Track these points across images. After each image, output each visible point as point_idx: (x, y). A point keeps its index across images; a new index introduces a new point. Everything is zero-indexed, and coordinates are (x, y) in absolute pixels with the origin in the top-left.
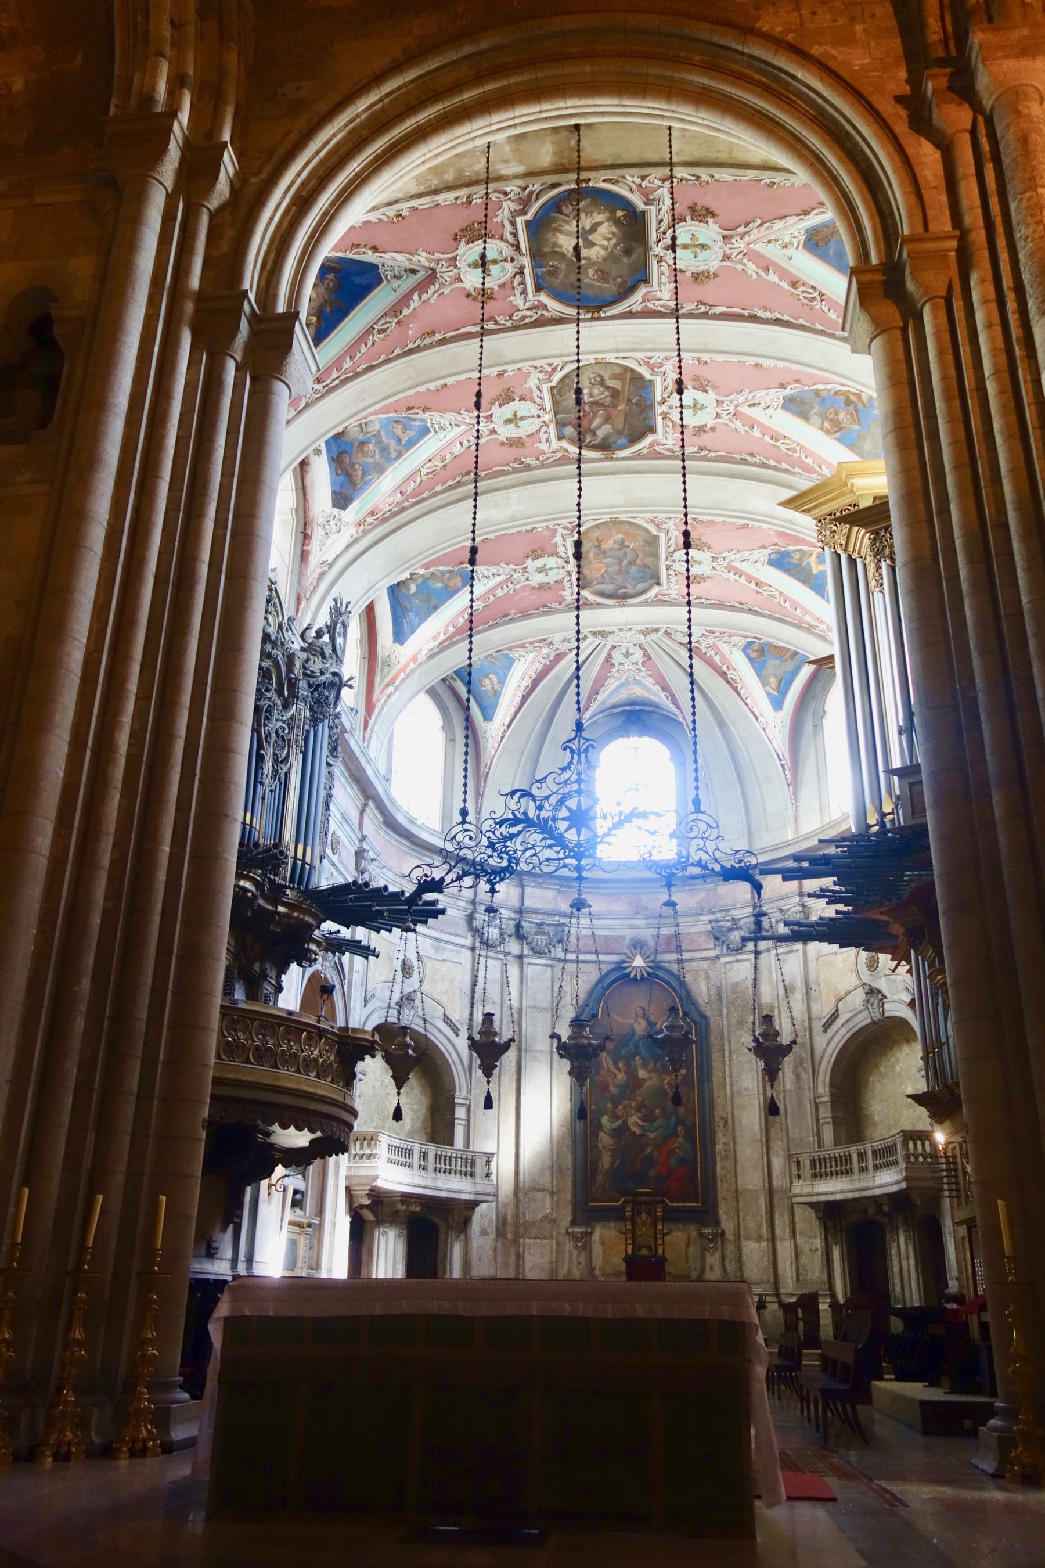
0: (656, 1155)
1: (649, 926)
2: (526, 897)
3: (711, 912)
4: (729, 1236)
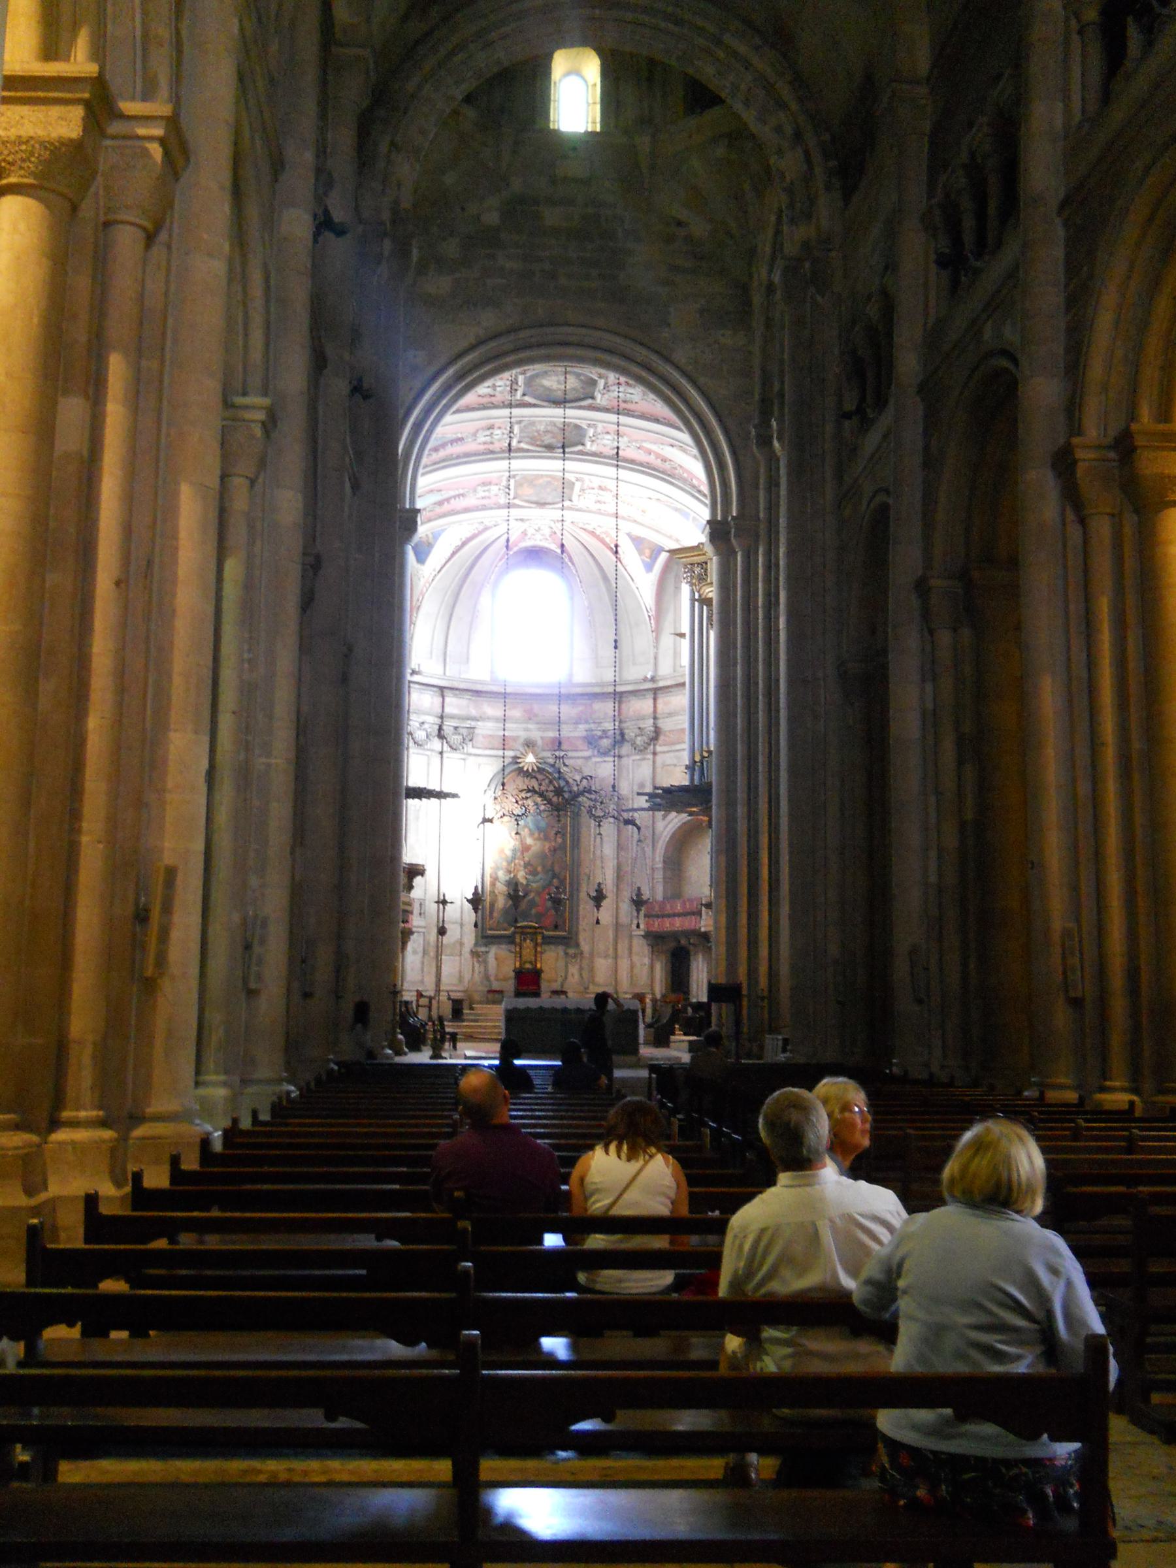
0: (537, 899)
1: (539, 729)
2: (445, 705)
3: (587, 722)
4: (586, 954)
